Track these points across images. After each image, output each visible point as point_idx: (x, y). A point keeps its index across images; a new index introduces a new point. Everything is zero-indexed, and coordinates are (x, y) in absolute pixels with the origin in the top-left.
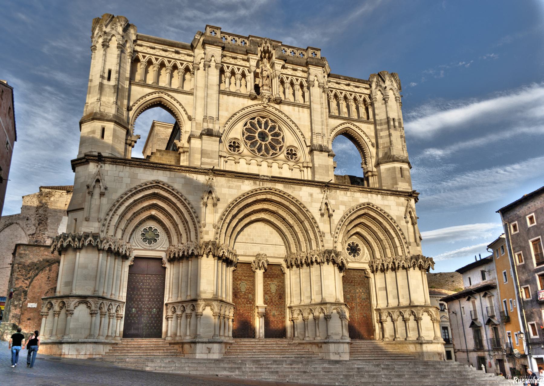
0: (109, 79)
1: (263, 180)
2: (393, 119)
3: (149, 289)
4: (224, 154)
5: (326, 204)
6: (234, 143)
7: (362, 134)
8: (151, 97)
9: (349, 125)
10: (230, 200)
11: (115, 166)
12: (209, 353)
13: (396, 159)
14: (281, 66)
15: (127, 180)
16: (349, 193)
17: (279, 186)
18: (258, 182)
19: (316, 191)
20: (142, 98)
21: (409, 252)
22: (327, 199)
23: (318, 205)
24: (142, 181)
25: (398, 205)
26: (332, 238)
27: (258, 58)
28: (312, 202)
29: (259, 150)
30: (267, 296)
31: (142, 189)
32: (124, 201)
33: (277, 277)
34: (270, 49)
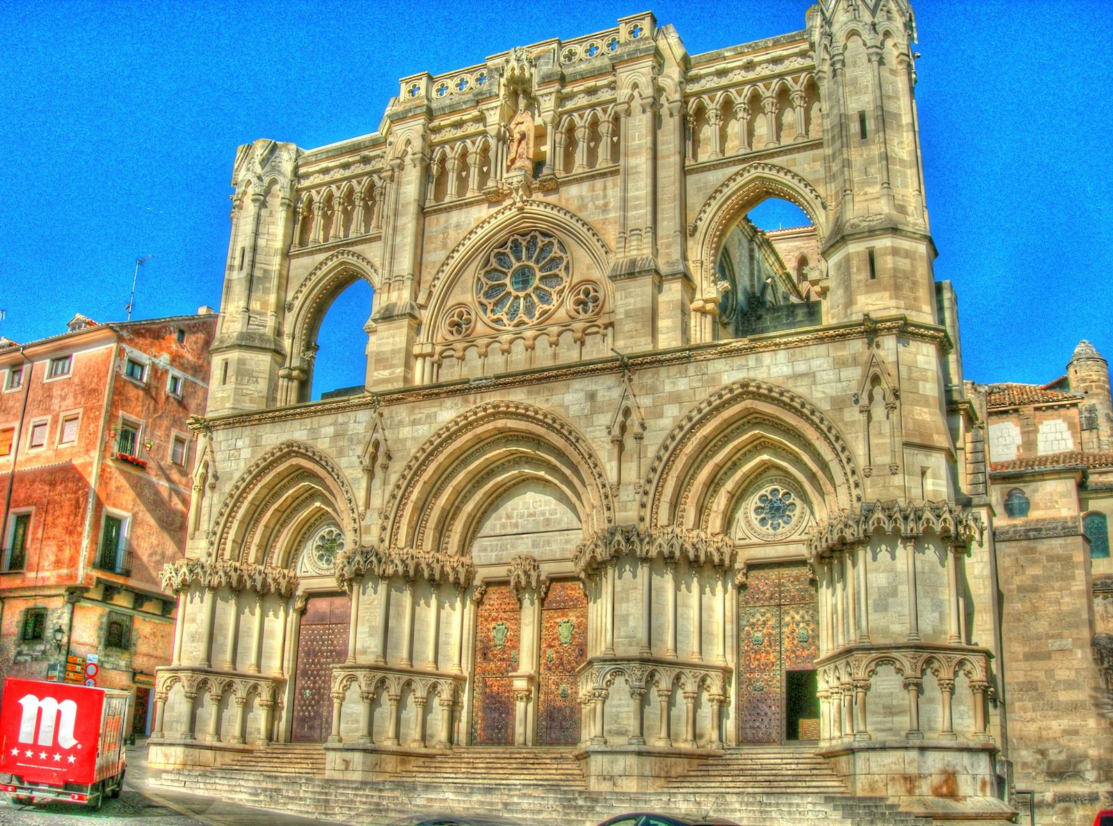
0: (241, 268)
1: (479, 389)
2: (862, 119)
3: (331, 652)
4: (427, 349)
6: (461, 315)
7: (794, 183)
8: (325, 269)
9: (759, 172)
12: (347, 769)
13: (846, 232)
14: (553, 96)
15: (246, 453)
16: (692, 368)
17: (518, 396)
18: (471, 397)
19: (608, 389)
20: (308, 279)
22: (624, 397)
23: (604, 419)
24: (268, 449)
25: (840, 364)
26: (638, 497)
27: (498, 104)
28: (593, 412)
29: (513, 313)
30: (550, 652)
33: (575, 606)
34: (517, 72)
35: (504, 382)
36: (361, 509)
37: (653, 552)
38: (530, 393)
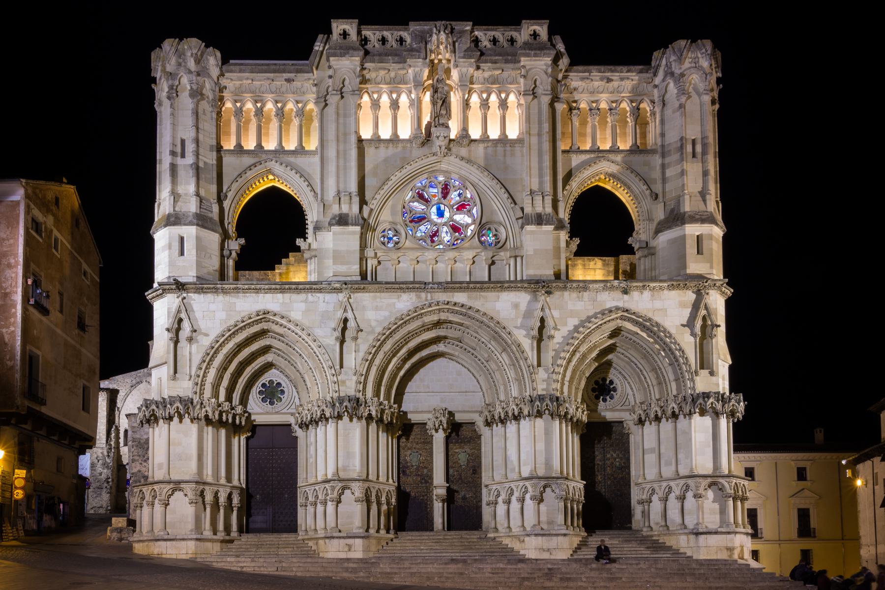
5: (542, 320)
10: (379, 329)
11: (202, 295)
16: (586, 294)
17: (460, 297)
18: (423, 295)
21: (694, 388)
22: (542, 309)
24: (243, 314)
31: (245, 326)
32: (221, 345)
35: (453, 285)
36: (338, 367)
37: (563, 413)
38: (469, 297)
